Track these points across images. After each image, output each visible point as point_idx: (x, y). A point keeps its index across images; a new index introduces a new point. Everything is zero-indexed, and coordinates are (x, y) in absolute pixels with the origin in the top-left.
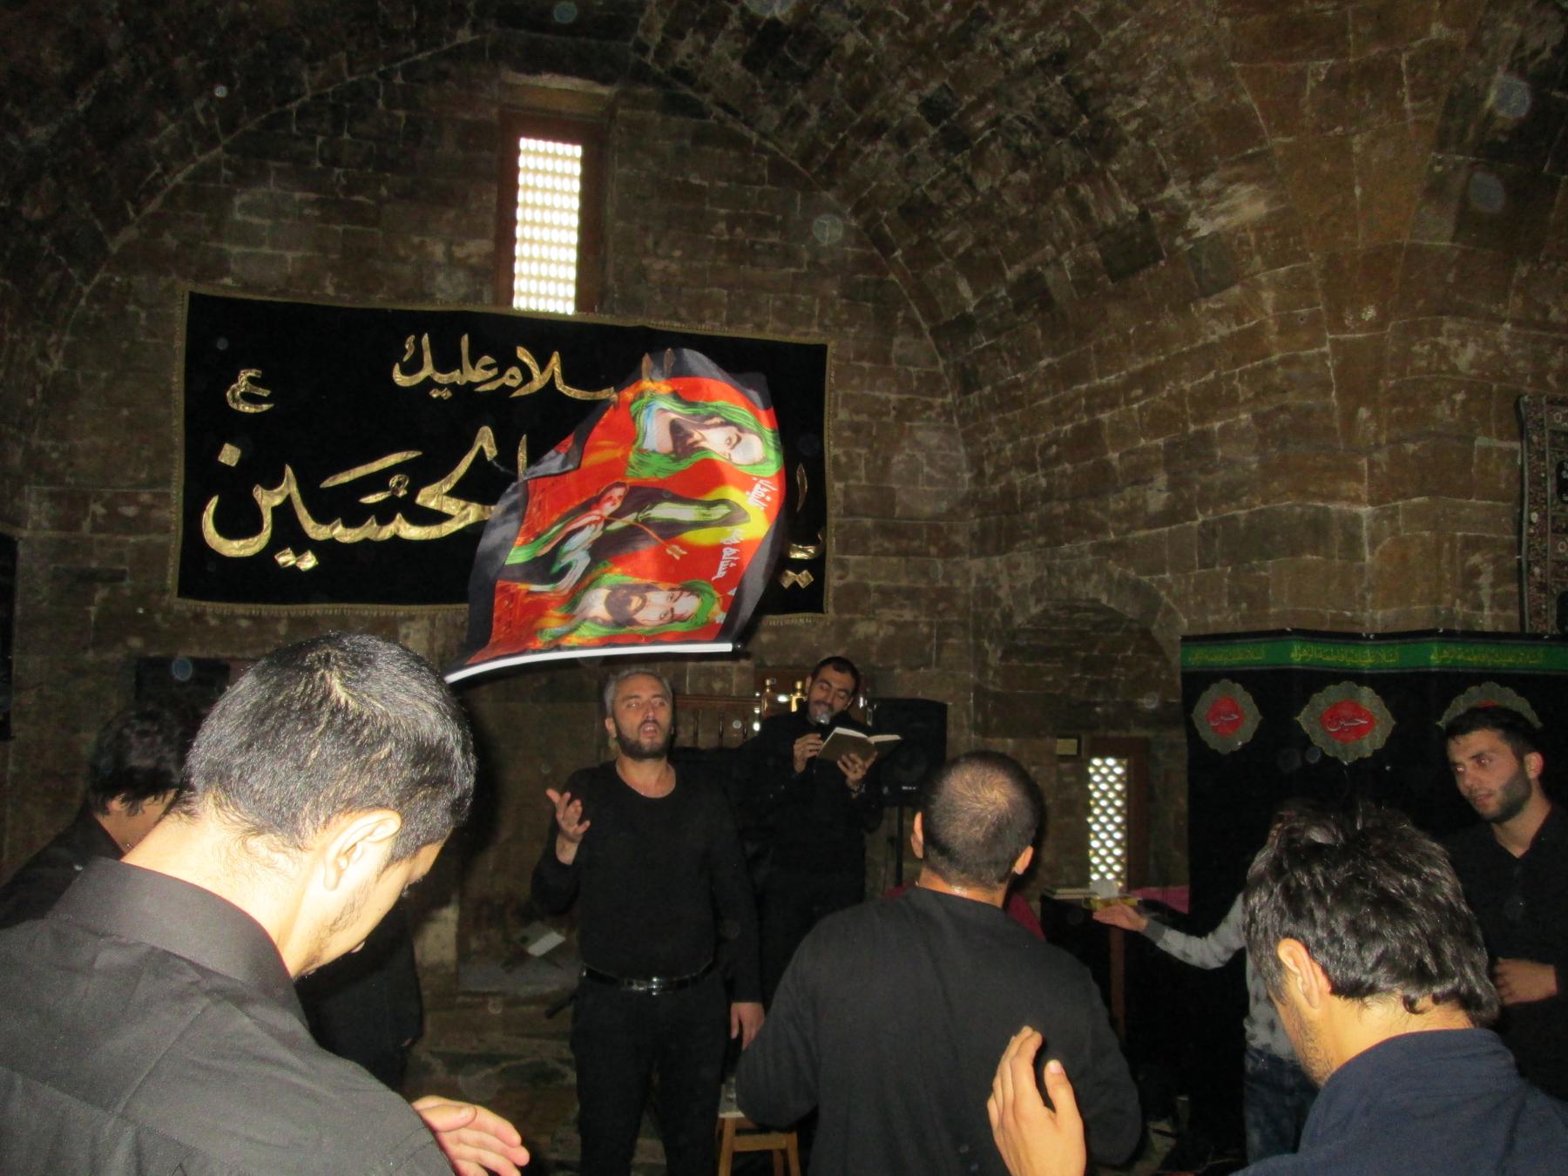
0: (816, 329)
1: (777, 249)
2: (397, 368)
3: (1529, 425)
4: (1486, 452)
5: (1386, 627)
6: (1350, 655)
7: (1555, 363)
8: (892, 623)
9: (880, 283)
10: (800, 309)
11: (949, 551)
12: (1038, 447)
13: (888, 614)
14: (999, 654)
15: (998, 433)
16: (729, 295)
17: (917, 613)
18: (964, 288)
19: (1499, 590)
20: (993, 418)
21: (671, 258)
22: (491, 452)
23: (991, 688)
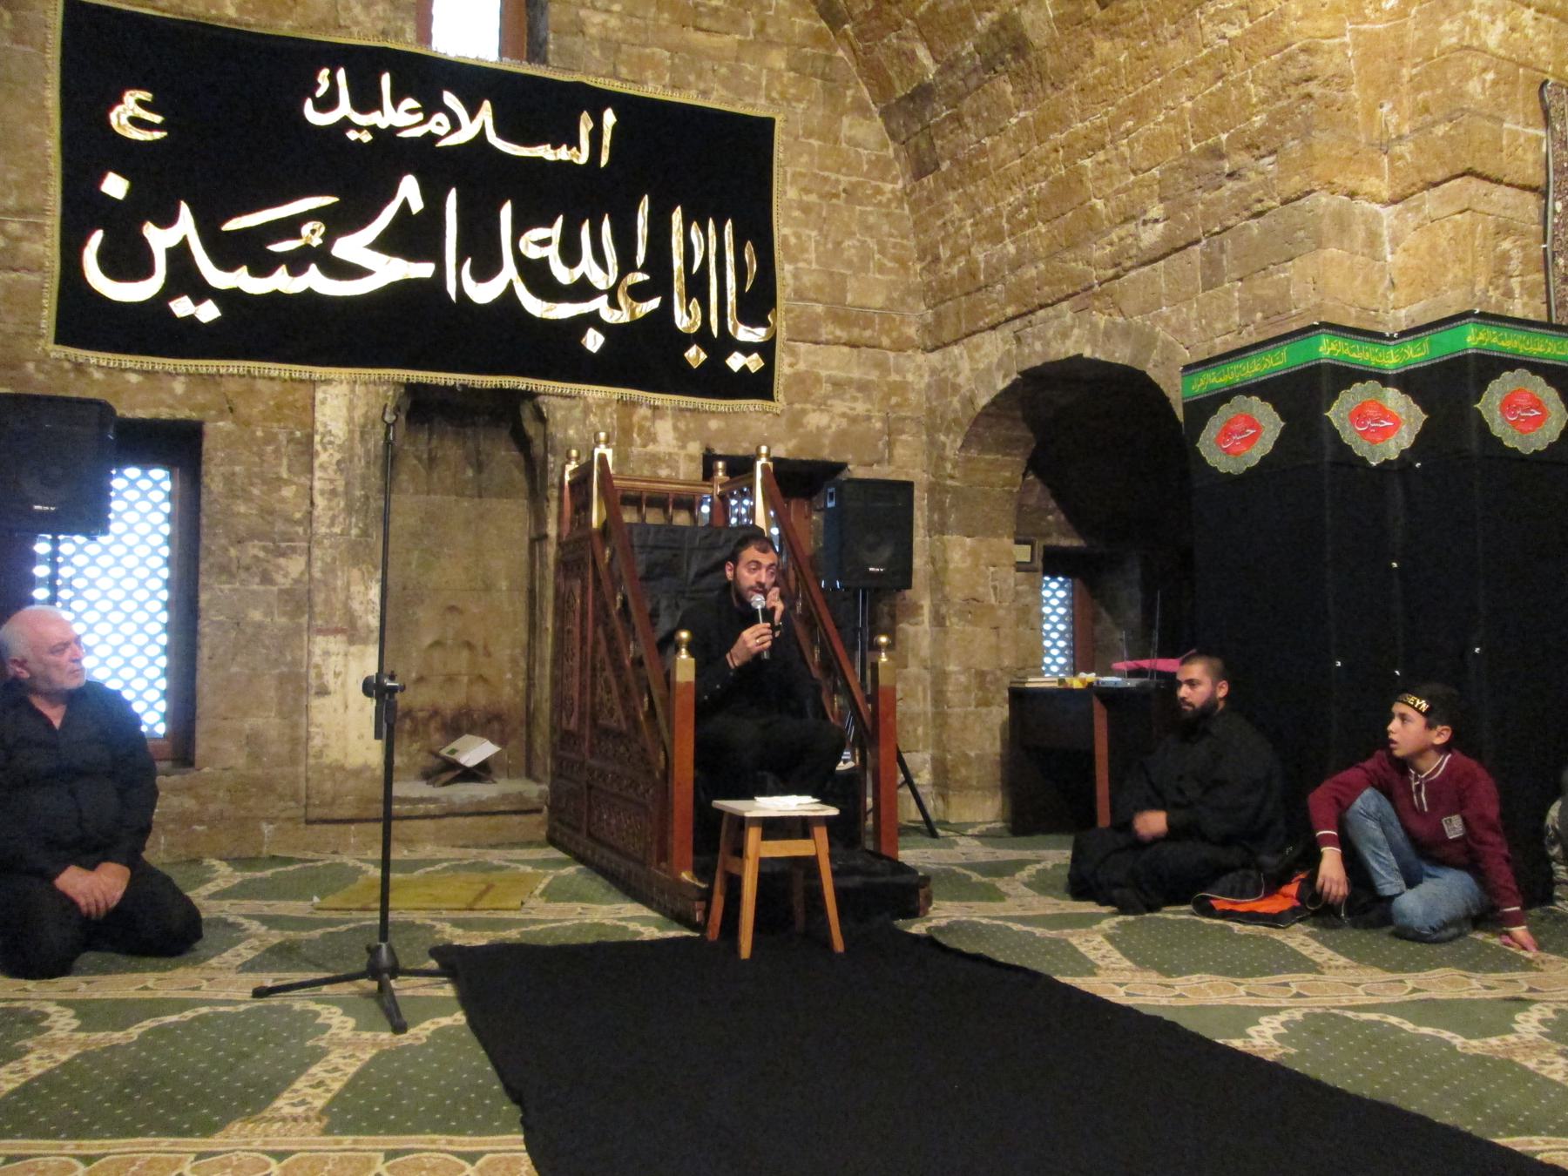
0: (762, 101)
1: (722, 14)
2: (309, 104)
3: (1552, 112)
4: (1515, 135)
5: (1413, 321)
6: (1375, 354)
8: (844, 415)
9: (828, 59)
10: (747, 79)
11: (900, 346)
12: (1005, 213)
13: (840, 406)
14: (959, 443)
15: (957, 211)
16: (672, 58)
17: (869, 406)
18: (922, 53)
19: (1529, 278)
20: (951, 197)
21: (608, 11)
22: (417, 205)
23: (949, 482)
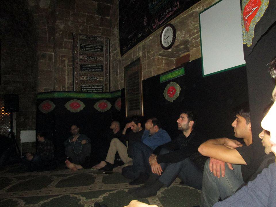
7: (81, 28)
